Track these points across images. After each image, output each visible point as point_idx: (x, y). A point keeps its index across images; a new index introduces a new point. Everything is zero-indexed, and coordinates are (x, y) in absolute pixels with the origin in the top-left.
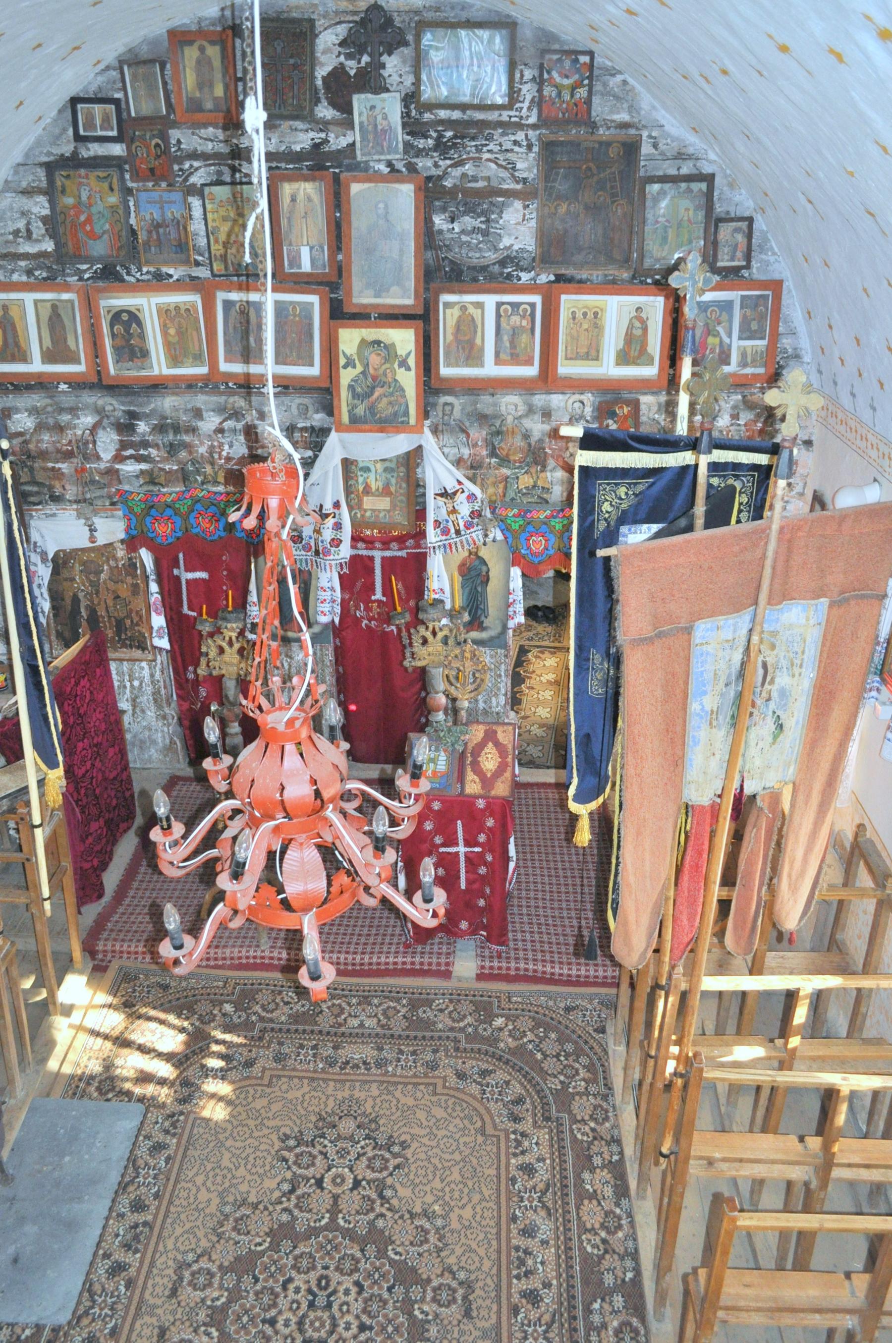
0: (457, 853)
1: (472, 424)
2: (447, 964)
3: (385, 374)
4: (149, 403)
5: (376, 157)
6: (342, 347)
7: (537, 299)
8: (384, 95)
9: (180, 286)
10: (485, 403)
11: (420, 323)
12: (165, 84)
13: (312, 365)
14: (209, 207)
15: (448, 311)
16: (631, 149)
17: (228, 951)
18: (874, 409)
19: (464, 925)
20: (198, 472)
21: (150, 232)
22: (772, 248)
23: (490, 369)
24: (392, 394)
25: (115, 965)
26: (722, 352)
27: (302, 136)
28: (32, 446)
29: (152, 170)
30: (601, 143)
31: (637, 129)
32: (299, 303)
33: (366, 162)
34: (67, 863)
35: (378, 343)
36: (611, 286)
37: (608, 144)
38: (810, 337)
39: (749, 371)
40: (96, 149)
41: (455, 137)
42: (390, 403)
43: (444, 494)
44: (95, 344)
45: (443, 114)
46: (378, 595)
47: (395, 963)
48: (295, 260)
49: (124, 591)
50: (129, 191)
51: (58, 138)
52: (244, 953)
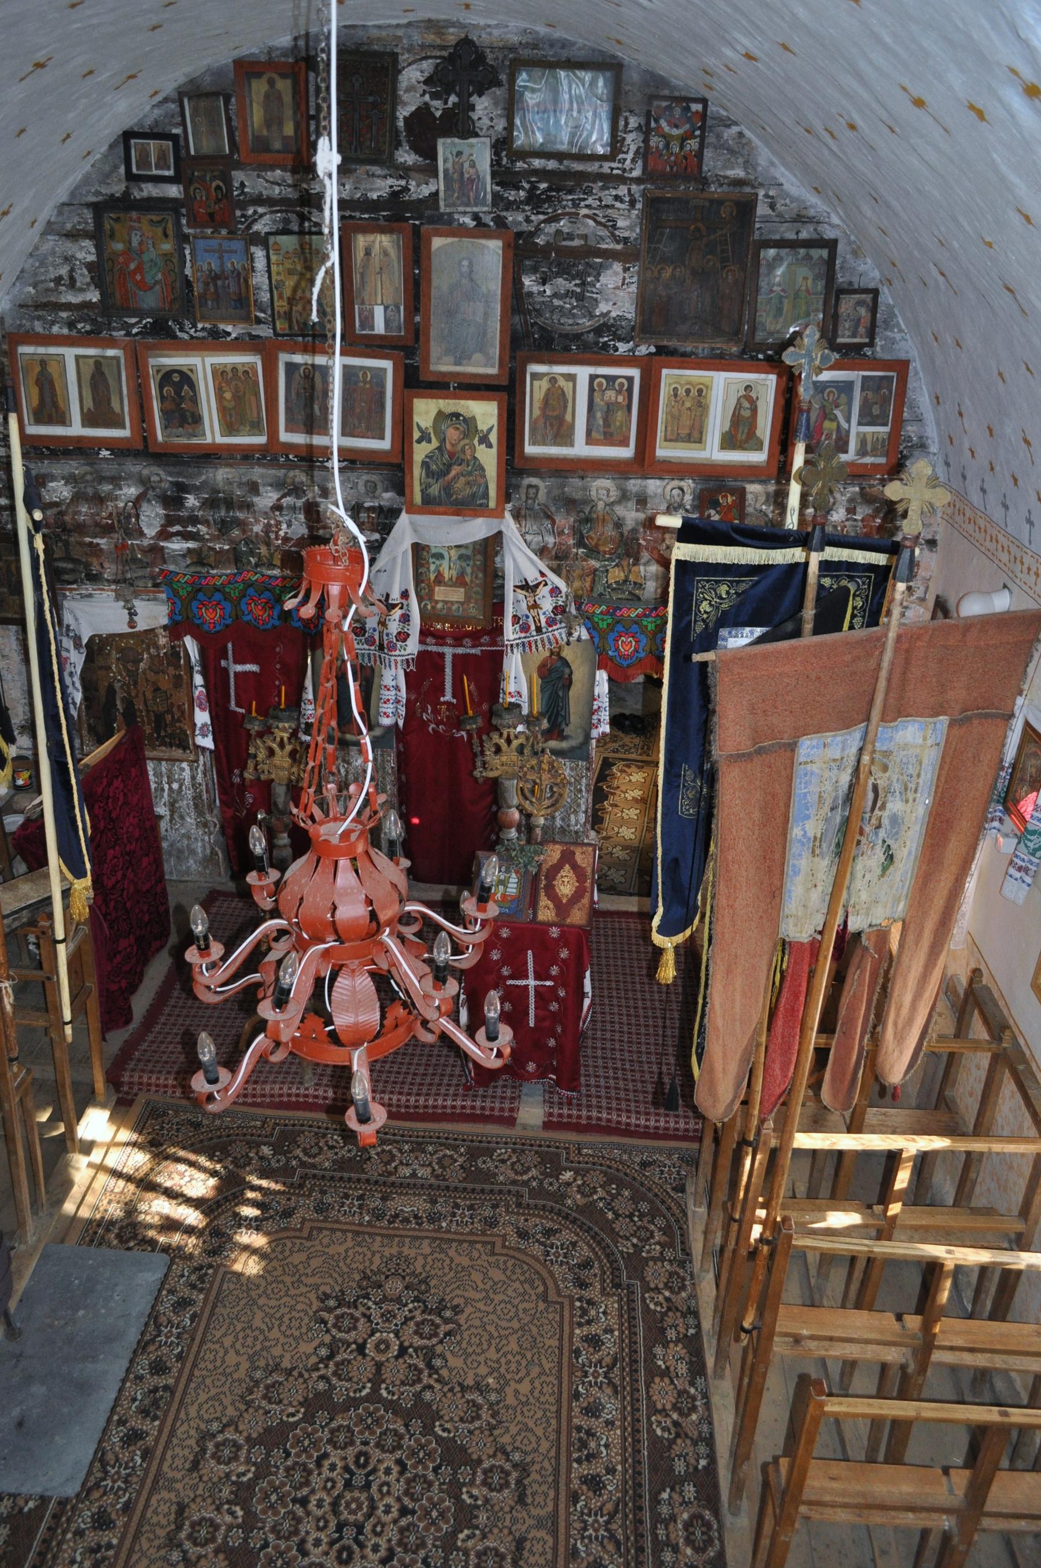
0: (526, 987)
1: (558, 510)
2: (512, 1110)
3: (463, 451)
4: (200, 474)
5: (461, 209)
6: (416, 419)
7: (635, 373)
8: (473, 140)
9: (239, 345)
10: (573, 486)
11: (504, 396)
12: (229, 120)
13: (382, 438)
14: (273, 258)
15: (536, 383)
16: (746, 208)
17: (268, 1087)
18: (1006, 507)
19: (531, 1067)
20: (252, 553)
21: (207, 284)
22: (898, 325)
23: (580, 449)
24: (470, 473)
25: (142, 1099)
26: (839, 438)
27: (379, 183)
28: (67, 518)
29: (211, 216)
30: (712, 201)
31: (753, 187)
32: (370, 369)
33: (450, 214)
34: (92, 984)
35: (457, 415)
36: (719, 361)
37: (720, 202)
38: (938, 424)
39: (868, 460)
40: (150, 190)
41: (550, 189)
42: (468, 483)
43: (525, 587)
44: (142, 406)
45: (537, 163)
46: (448, 697)
47: (454, 1107)
48: (368, 321)
49: (165, 682)
50: (185, 238)
51: (108, 175)
52: (285, 1090)
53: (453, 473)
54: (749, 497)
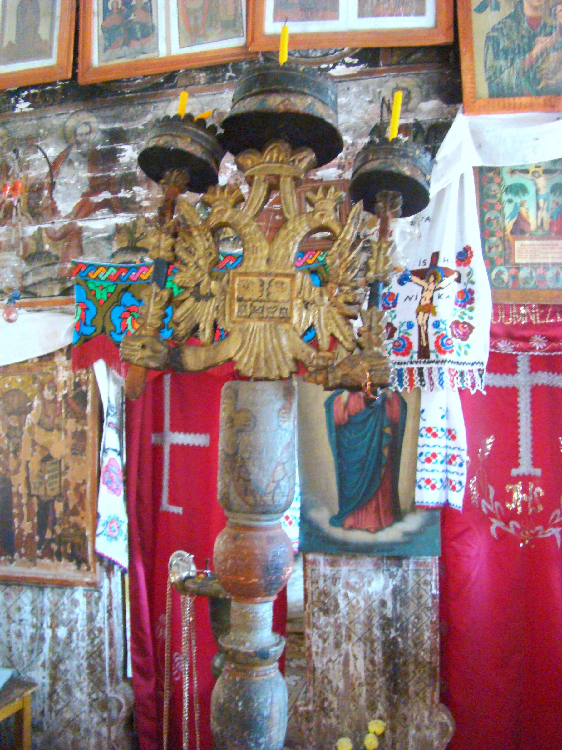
46: (525, 465)
53: (536, 51)
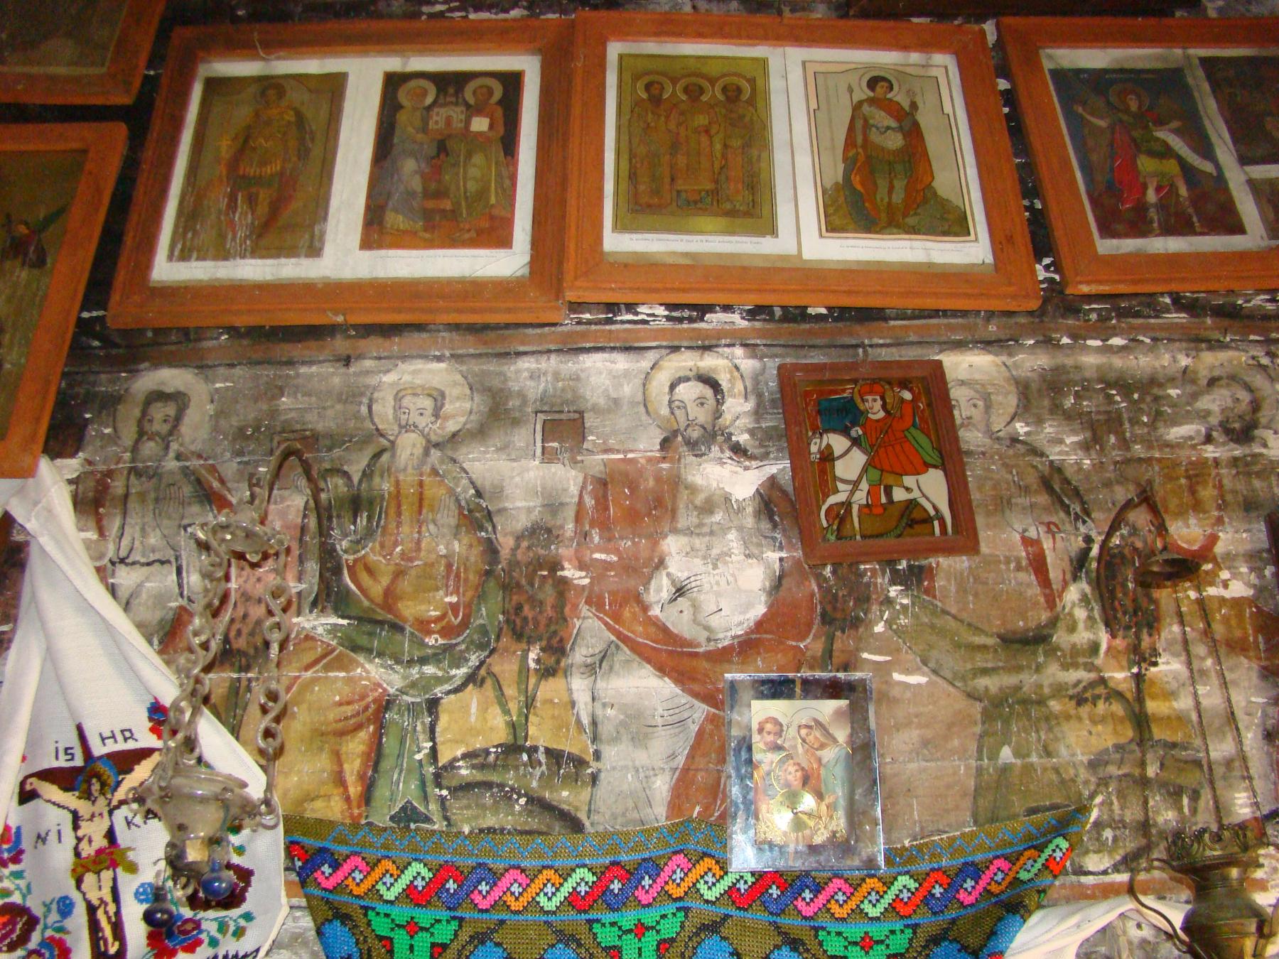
23: (343, 254)
26: (1199, 199)
54: (956, 393)
